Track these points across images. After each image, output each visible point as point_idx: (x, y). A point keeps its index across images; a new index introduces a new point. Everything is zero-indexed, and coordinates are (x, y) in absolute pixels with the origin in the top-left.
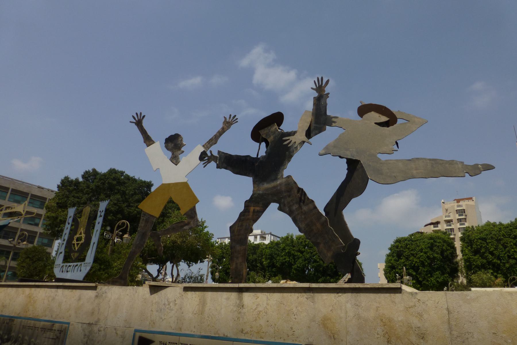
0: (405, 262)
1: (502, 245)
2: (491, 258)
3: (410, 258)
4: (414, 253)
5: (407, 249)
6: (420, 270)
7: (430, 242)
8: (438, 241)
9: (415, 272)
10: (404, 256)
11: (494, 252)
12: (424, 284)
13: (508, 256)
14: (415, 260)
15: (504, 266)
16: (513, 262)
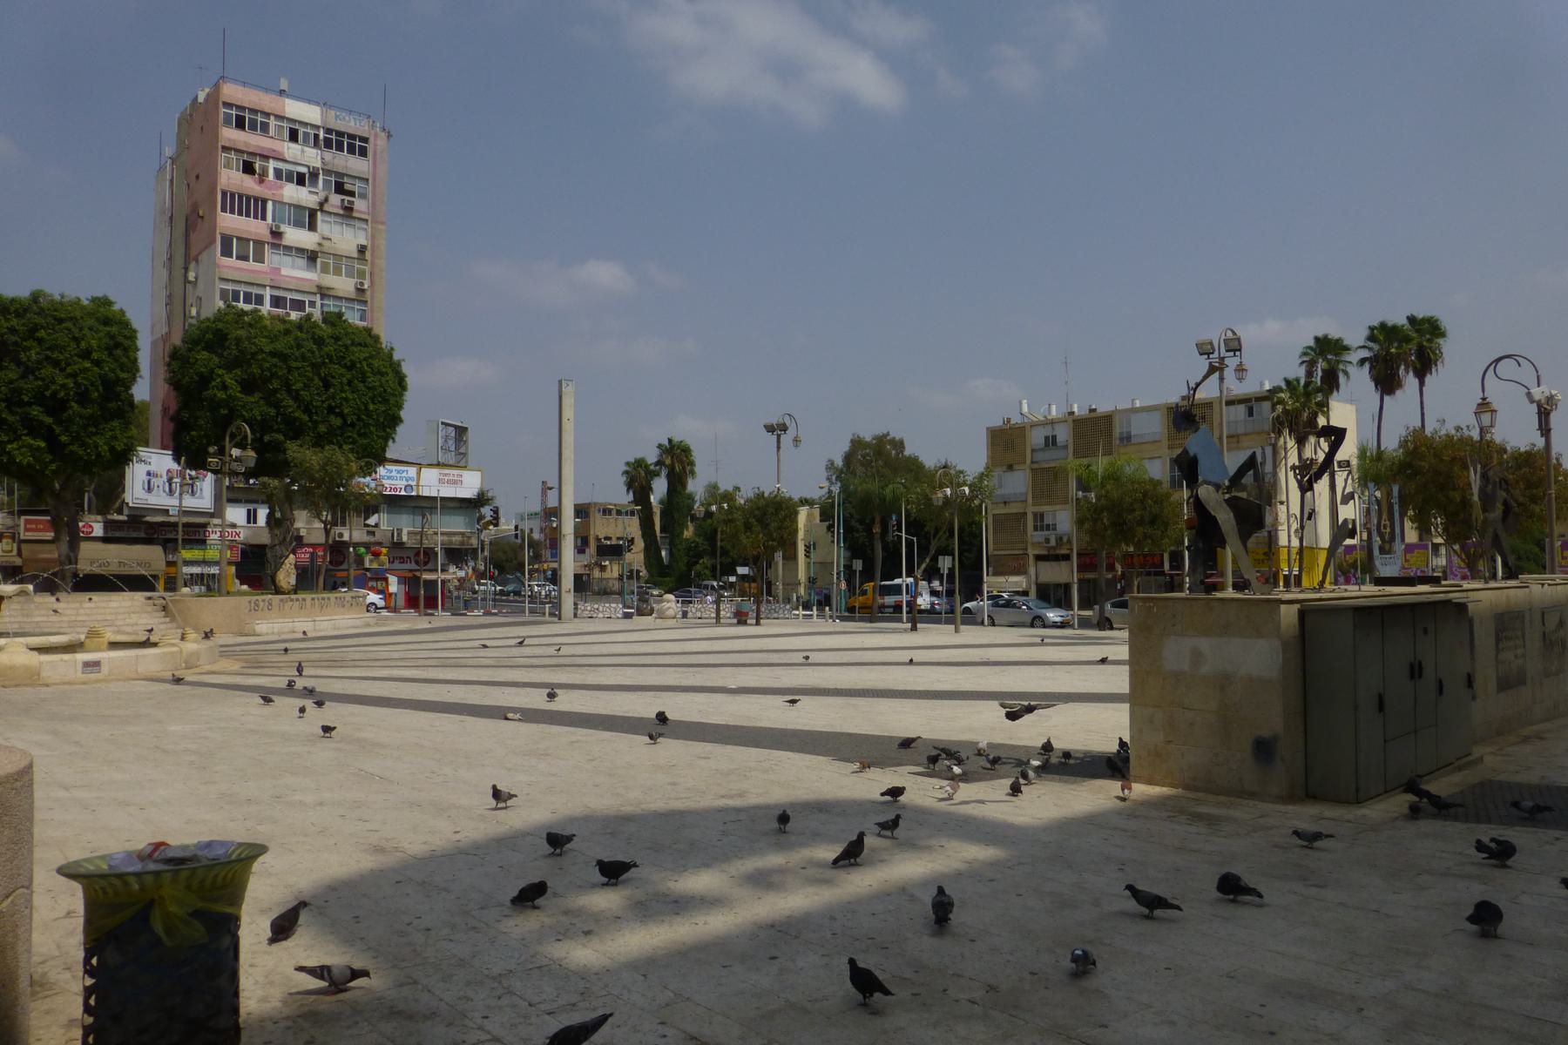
0: (16, 380)
1: (321, 379)
2: (290, 406)
3: (43, 371)
4: (62, 357)
5: (34, 339)
6: (71, 412)
7: (109, 332)
8: (126, 332)
9: (49, 415)
10: (19, 363)
11: (302, 393)
12: (71, 451)
13: (330, 405)
14: (60, 380)
15: (315, 428)
16: (337, 422)
